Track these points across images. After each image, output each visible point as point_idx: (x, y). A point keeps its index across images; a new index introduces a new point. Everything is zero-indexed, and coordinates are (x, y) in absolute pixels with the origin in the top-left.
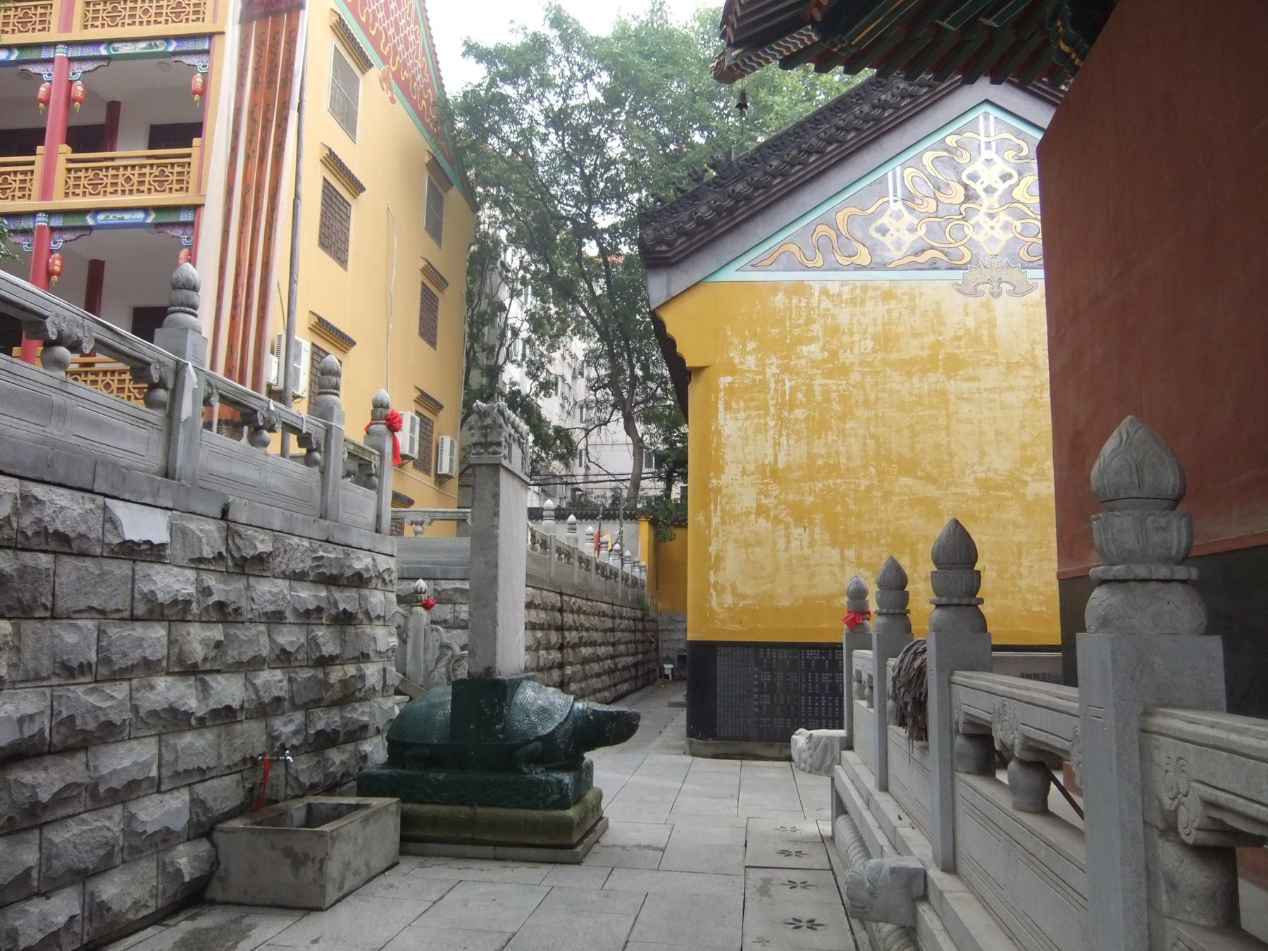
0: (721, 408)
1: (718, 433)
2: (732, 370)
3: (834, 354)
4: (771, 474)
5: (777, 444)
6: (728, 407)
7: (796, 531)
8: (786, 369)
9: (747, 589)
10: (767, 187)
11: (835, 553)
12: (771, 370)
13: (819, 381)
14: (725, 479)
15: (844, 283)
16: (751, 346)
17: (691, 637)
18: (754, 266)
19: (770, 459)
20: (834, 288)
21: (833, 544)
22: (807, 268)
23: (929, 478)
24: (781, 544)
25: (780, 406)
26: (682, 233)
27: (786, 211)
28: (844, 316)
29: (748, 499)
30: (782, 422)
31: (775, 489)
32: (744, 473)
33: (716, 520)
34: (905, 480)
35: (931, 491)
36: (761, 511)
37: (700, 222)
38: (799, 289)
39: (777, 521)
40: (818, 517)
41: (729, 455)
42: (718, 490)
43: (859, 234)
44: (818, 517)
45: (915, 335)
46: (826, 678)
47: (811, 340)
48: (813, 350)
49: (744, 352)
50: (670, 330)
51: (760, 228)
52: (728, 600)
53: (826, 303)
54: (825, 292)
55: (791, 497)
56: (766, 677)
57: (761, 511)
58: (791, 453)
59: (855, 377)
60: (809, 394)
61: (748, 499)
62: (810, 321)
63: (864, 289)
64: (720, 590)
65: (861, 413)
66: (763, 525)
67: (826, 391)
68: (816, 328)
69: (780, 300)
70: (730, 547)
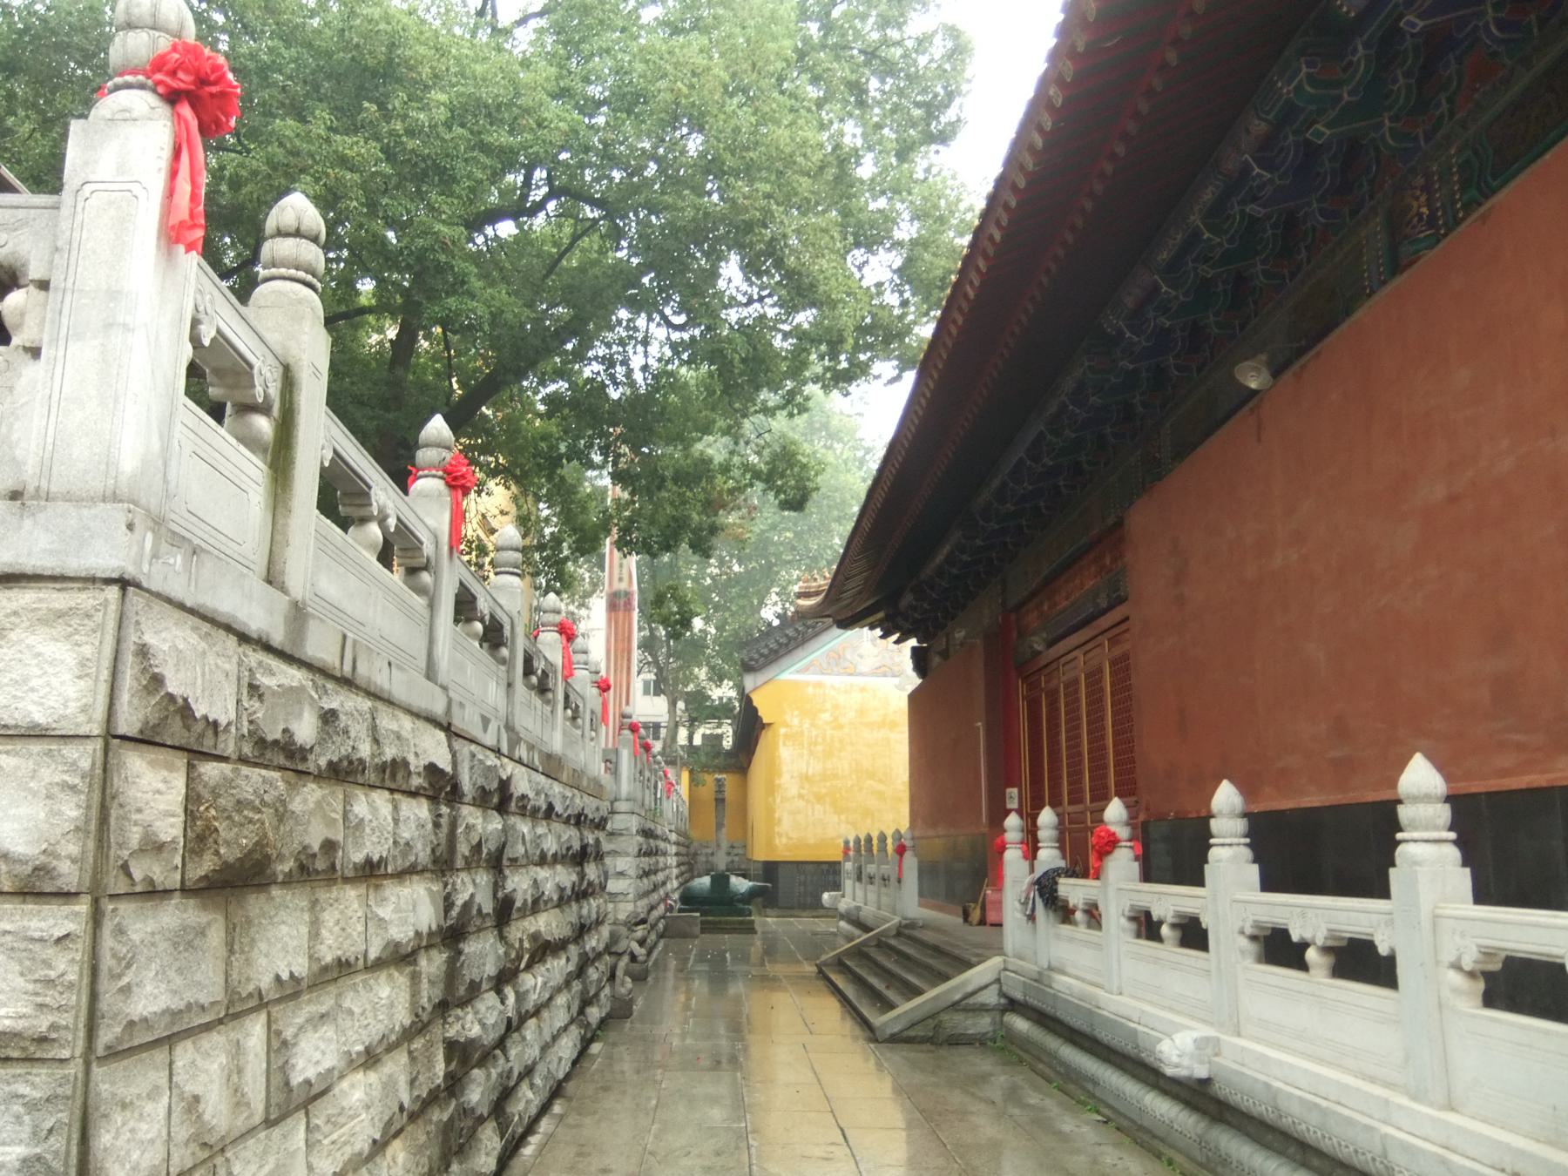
0: (781, 743)
2: (787, 725)
3: (836, 719)
4: (805, 778)
5: (808, 764)
6: (784, 744)
8: (812, 725)
9: (794, 835)
11: (835, 818)
13: (829, 732)
16: (796, 713)
23: (880, 781)
24: (810, 813)
26: (762, 655)
27: (813, 644)
30: (811, 753)
31: (807, 786)
33: (778, 800)
34: (870, 782)
35: (881, 787)
36: (801, 796)
37: (771, 650)
38: (819, 685)
39: (808, 801)
41: (785, 769)
42: (779, 785)
43: (848, 657)
44: (828, 799)
46: (831, 878)
48: (826, 716)
50: (755, 704)
51: (800, 652)
52: (784, 840)
54: (832, 687)
56: (802, 878)
57: (801, 796)
58: (815, 767)
61: (793, 790)
64: (780, 835)
66: (801, 804)
68: (828, 705)
69: (810, 690)
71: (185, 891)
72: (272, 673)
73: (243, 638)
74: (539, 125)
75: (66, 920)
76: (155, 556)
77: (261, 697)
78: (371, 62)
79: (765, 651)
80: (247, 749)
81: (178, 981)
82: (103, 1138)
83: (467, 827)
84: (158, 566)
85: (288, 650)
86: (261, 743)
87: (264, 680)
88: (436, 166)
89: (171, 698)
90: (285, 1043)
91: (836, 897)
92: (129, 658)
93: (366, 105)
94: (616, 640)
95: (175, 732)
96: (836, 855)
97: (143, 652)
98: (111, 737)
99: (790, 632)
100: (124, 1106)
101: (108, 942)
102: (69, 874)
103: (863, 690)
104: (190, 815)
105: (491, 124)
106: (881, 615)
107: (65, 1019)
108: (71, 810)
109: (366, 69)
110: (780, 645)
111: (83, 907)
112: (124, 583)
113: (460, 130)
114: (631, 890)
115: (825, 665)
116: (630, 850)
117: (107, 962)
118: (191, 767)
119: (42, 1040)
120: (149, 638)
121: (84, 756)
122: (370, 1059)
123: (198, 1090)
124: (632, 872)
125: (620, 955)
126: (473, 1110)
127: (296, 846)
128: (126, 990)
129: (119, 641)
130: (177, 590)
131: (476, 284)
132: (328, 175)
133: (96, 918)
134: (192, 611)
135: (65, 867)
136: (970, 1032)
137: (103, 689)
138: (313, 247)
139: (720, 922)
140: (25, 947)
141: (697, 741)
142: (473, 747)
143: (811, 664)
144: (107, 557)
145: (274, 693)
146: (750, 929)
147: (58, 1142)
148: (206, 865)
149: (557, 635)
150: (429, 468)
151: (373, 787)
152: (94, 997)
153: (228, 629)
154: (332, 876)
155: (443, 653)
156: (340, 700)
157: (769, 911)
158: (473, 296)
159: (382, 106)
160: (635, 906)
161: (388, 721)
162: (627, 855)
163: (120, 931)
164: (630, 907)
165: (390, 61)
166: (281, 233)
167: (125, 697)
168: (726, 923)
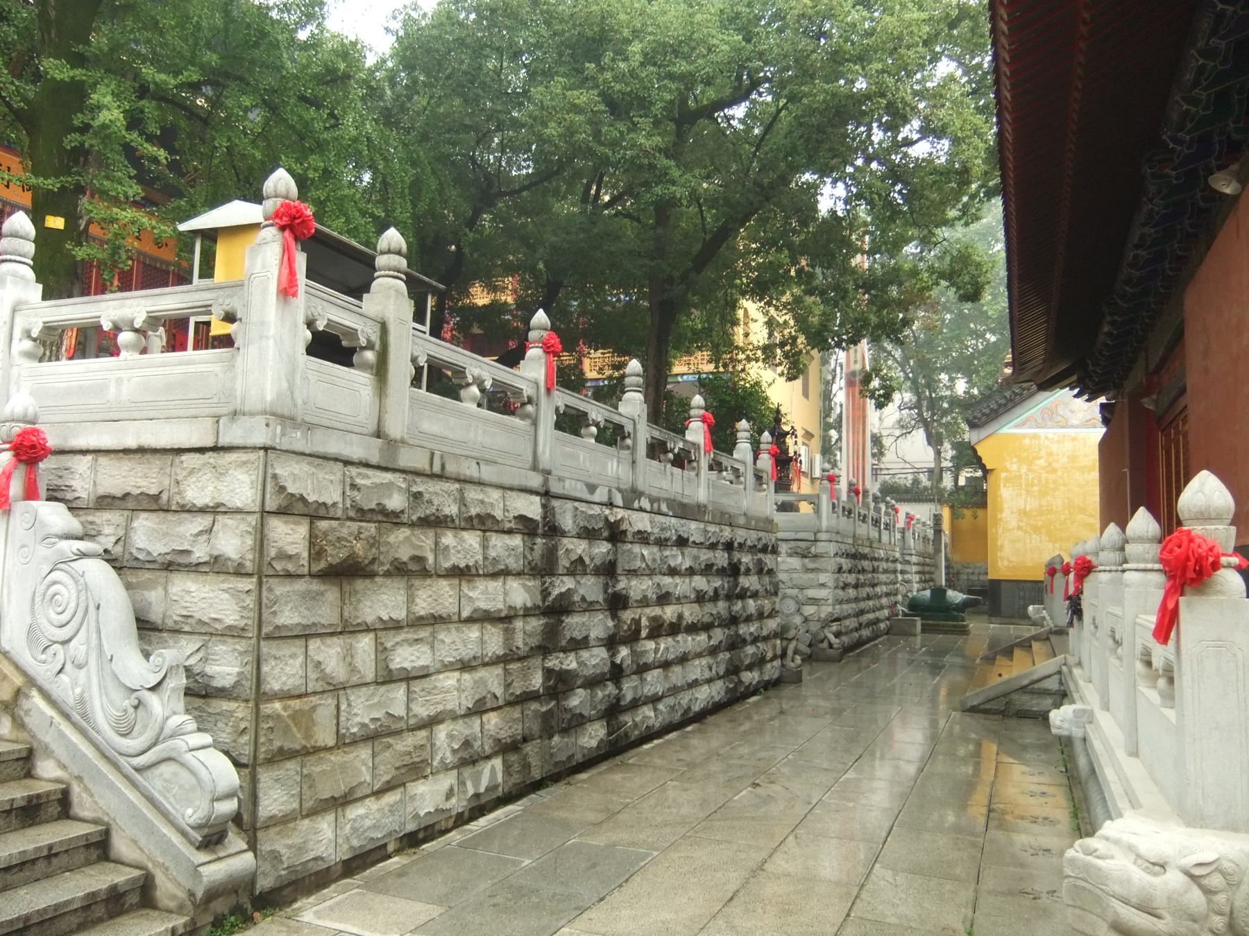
1: (1001, 496)
2: (1007, 471)
3: (1050, 464)
4: (1024, 513)
5: (1026, 501)
6: (1005, 486)
7: (1034, 536)
8: (1029, 470)
10: (1021, 395)
12: (1023, 470)
13: (1044, 475)
14: (1004, 515)
15: (1055, 434)
16: (1015, 460)
17: (989, 577)
18: (1016, 427)
19: (1023, 507)
20: (1050, 436)
21: (1050, 541)
22: (1039, 427)
24: (1028, 541)
25: (1027, 485)
26: (984, 414)
28: (1055, 448)
29: (1013, 523)
30: (1028, 491)
31: (1025, 519)
32: (1012, 513)
36: (1019, 528)
37: (992, 410)
38: (1035, 437)
39: (1026, 532)
40: (1043, 531)
41: (1005, 505)
42: (1001, 519)
43: (1061, 413)
44: (1043, 531)
45: (1086, 456)
47: (1041, 458)
48: (1042, 462)
49: (1012, 463)
50: (979, 454)
51: (1017, 410)
52: (1006, 563)
53: (1047, 443)
54: (1046, 438)
55: (1032, 522)
56: (1022, 594)
57: (1019, 528)
58: (1032, 504)
59: (1060, 473)
60: (1040, 481)
61: (1013, 523)
62: (1040, 450)
63: (1064, 436)
65: (1062, 488)
66: (1020, 533)
67: (1047, 479)
68: (1043, 453)
69: (1027, 441)
70: (1006, 542)
71: (311, 575)
72: (368, 477)
73: (347, 463)
74: (710, 50)
75: (249, 584)
76: (283, 434)
77: (359, 490)
78: (589, 34)
79: (987, 411)
80: (352, 514)
81: (306, 613)
82: (265, 669)
83: (567, 550)
84: (284, 439)
85: (383, 464)
86: (360, 510)
87: (359, 481)
88: (637, 97)
89: (292, 495)
90: (385, 649)
91: (1039, 609)
92: (269, 480)
93: (587, 65)
94: (853, 409)
95: (300, 507)
96: (1040, 575)
97: (275, 476)
98: (264, 513)
99: (1007, 394)
100: (275, 658)
101: (265, 593)
102: (249, 567)
103: (1074, 439)
104: (311, 544)
105: (676, 57)
106: (1075, 378)
107: (250, 622)
108: (249, 541)
109: (588, 39)
110: (1000, 405)
111: (254, 580)
112: (266, 449)
113: (652, 68)
114: (830, 597)
115: (1040, 421)
116: (829, 568)
117: (264, 601)
118: (311, 523)
119: (243, 629)
120: (278, 471)
121: (253, 520)
122: (465, 666)
123: (321, 659)
124: (831, 584)
125: (790, 640)
126: (571, 710)
127: (390, 558)
128: (274, 613)
129: (265, 472)
130: (299, 447)
131: (675, 173)
132: (565, 120)
133: (260, 584)
134: (310, 455)
135: (248, 564)
136: (1035, 709)
137: (259, 493)
138: (397, 257)
139: (938, 625)
140: (235, 593)
141: (962, 482)
142: (576, 504)
143: (1028, 420)
144: (260, 438)
145: (368, 487)
146: (964, 631)
147: (248, 668)
148: (322, 565)
149: (700, 424)
150: (534, 342)
151: (463, 529)
152: (260, 615)
153: (336, 460)
154: (425, 573)
155: (544, 452)
156: (421, 486)
157: (993, 619)
158: (674, 183)
159: (598, 65)
160: (834, 609)
161: (473, 494)
162: (827, 571)
163: (270, 590)
164: (830, 609)
165: (603, 30)
166: (382, 253)
167: (268, 496)
168: (943, 626)
